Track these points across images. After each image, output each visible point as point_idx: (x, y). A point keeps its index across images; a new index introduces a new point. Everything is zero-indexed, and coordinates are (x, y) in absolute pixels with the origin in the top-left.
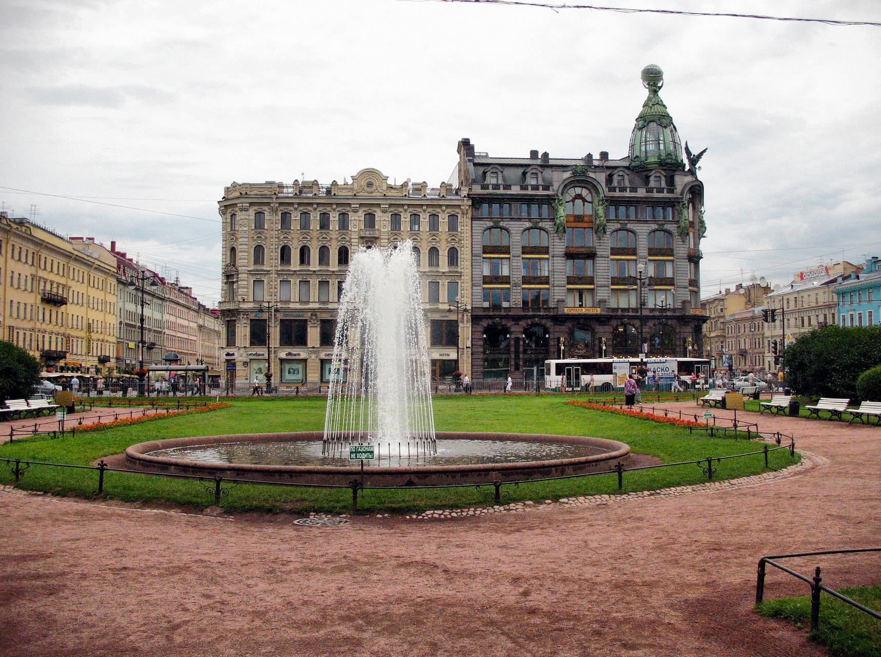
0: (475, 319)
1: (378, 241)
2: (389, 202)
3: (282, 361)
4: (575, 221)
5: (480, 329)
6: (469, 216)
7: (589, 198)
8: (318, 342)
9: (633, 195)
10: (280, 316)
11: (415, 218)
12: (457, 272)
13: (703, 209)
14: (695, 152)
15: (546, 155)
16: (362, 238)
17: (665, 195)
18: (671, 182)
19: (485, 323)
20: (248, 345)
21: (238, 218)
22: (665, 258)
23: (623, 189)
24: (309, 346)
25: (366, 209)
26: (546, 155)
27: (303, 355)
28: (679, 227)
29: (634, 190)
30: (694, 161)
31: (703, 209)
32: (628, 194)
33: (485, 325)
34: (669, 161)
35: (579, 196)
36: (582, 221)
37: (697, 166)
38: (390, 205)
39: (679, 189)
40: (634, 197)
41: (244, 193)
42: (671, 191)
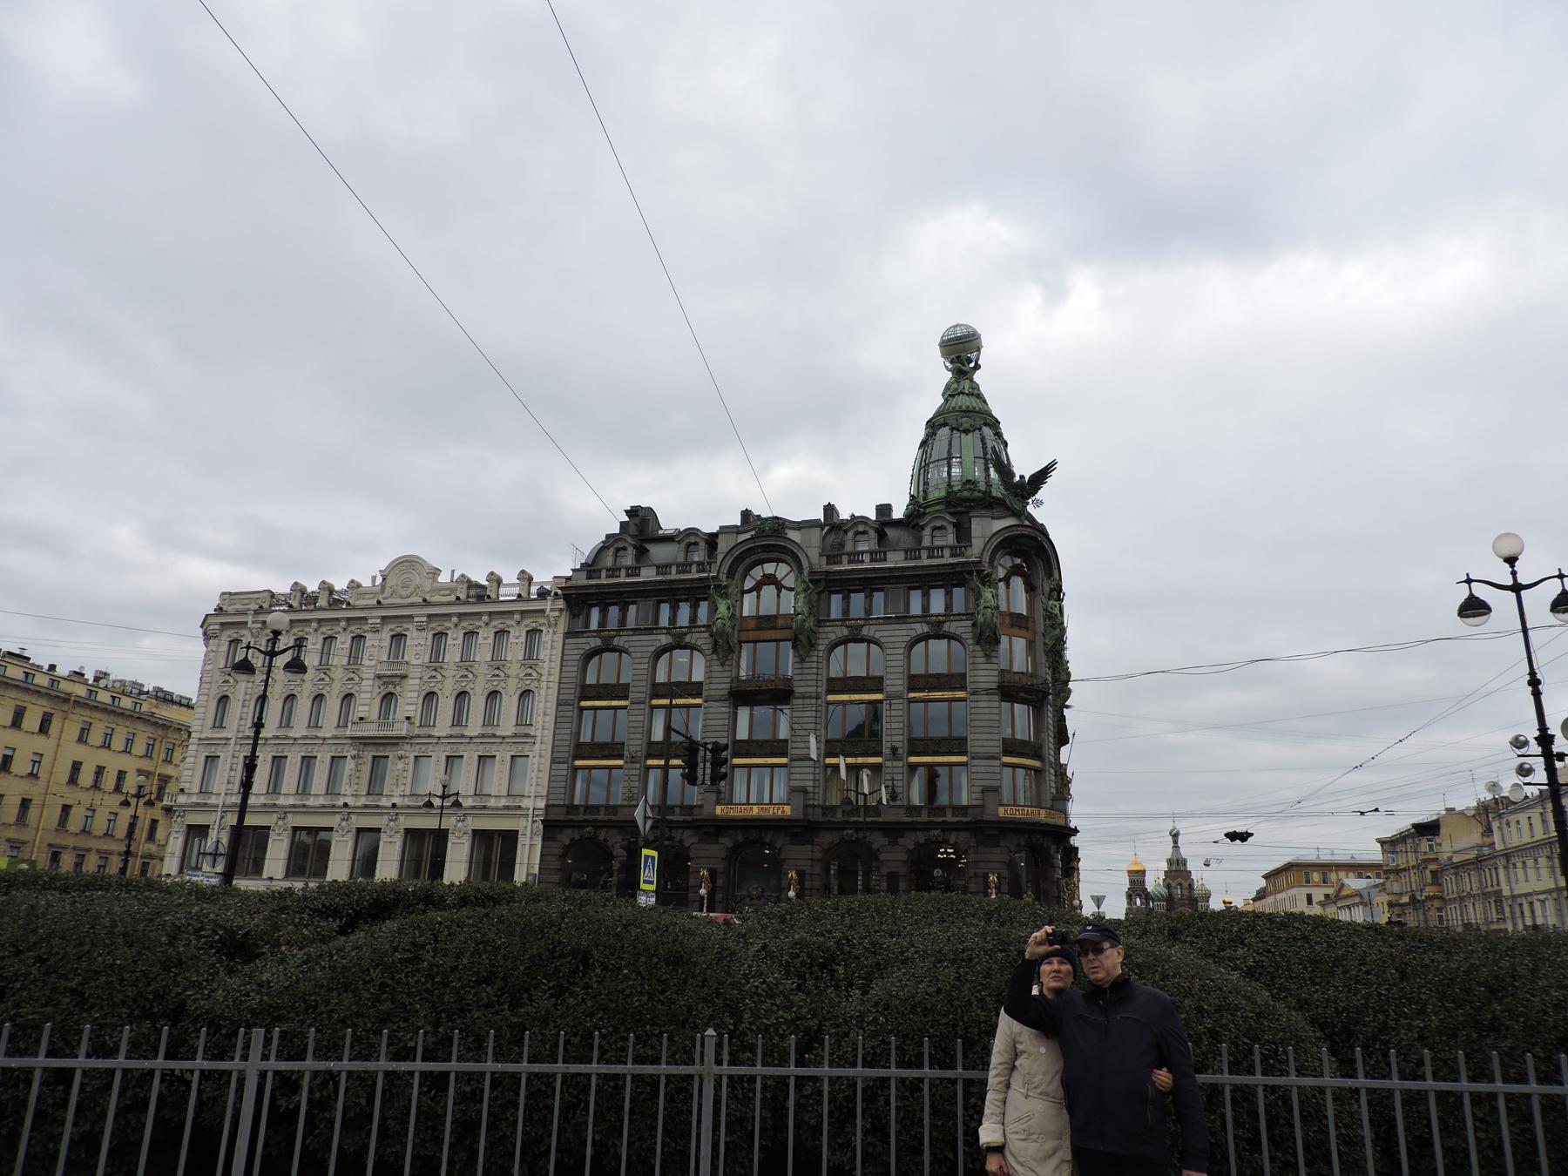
0: (551, 827)
1: (405, 682)
4: (758, 629)
5: (556, 848)
6: (562, 627)
7: (789, 582)
12: (527, 735)
16: (379, 677)
18: (963, 534)
19: (565, 837)
22: (947, 695)
24: (265, 876)
25: (392, 626)
28: (974, 625)
33: (567, 842)
34: (966, 494)
35: (769, 579)
36: (775, 628)
39: (977, 545)
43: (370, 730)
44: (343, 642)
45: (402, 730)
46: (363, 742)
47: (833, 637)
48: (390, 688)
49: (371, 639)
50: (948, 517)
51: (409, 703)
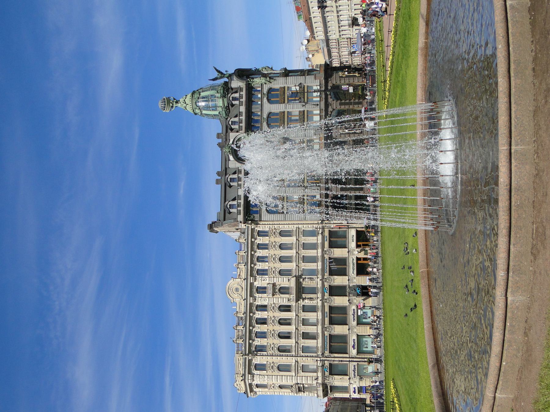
2: (249, 277)
3: (358, 352)
8: (344, 277)
9: (244, 114)
10: (327, 353)
11: (261, 259)
13: (254, 69)
14: (216, 74)
15: (218, 174)
16: (273, 295)
17: (244, 93)
20: (348, 377)
21: (259, 383)
23: (241, 122)
26: (218, 174)
27: (355, 337)
28: (265, 83)
29: (240, 114)
30: (222, 75)
31: (254, 69)
32: (243, 118)
37: (225, 73)
38: (251, 276)
40: (246, 113)
41: (241, 378)
42: (241, 89)
43: (293, 296)
44: (259, 315)
45: (292, 283)
46: (298, 298)
47: (266, 127)
48: (277, 290)
49: (259, 302)
50: (229, 95)
51: (283, 282)
